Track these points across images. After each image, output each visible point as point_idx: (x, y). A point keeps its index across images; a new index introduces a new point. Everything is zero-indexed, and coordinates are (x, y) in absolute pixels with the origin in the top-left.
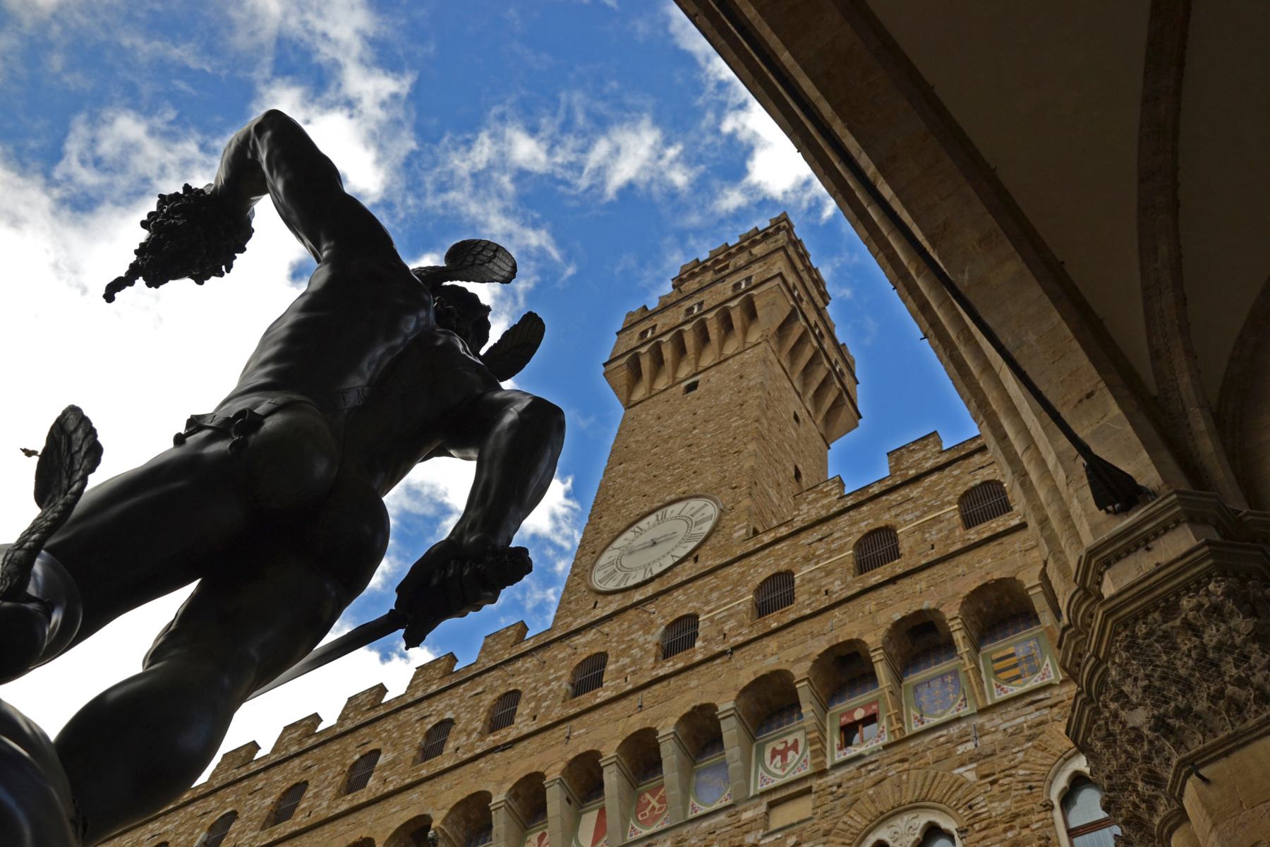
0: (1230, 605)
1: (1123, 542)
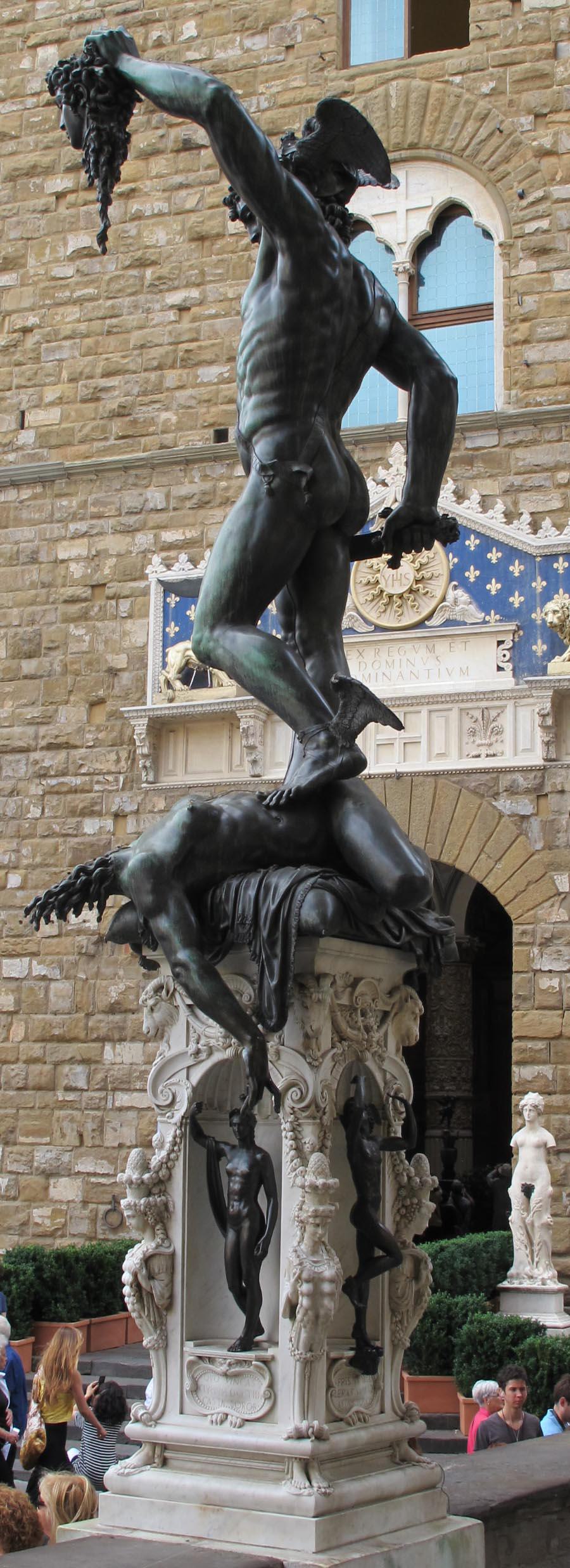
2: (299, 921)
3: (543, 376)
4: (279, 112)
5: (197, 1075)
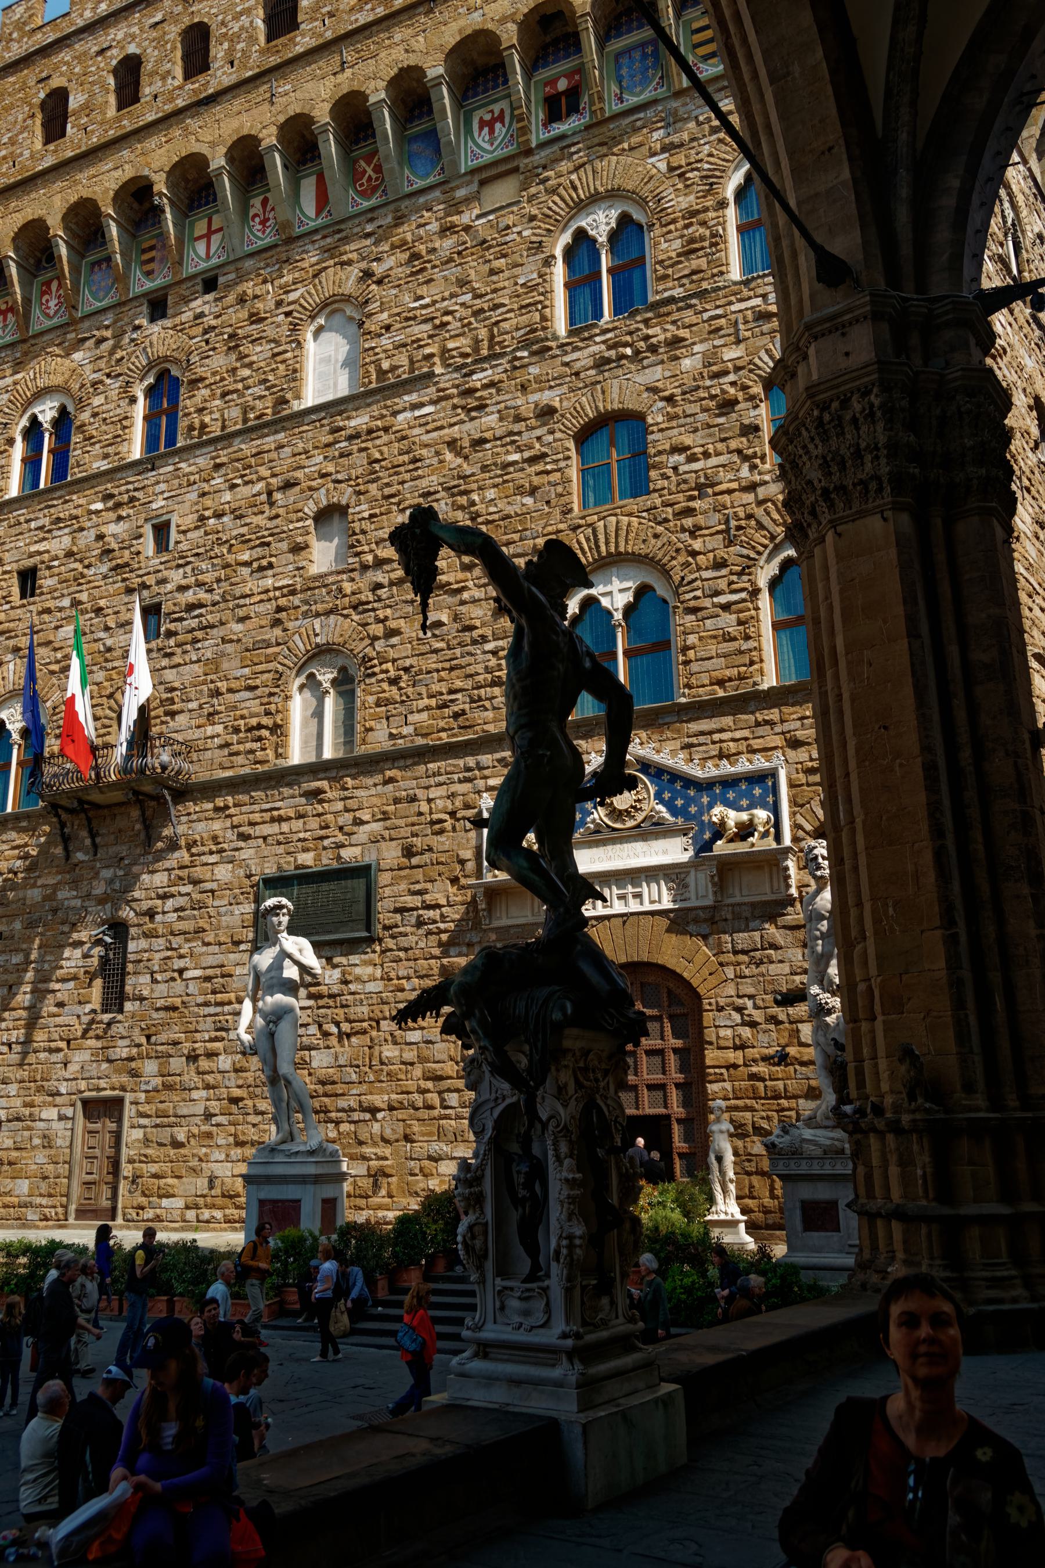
0: (879, 414)
1: (827, 325)
4: (520, 551)
5: (496, 1113)
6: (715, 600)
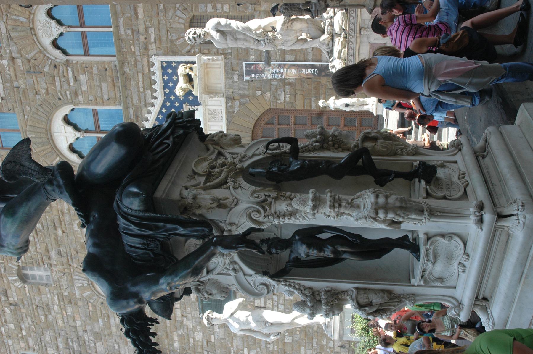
2: (140, 211)
3: (112, 94)
6: (71, 84)
